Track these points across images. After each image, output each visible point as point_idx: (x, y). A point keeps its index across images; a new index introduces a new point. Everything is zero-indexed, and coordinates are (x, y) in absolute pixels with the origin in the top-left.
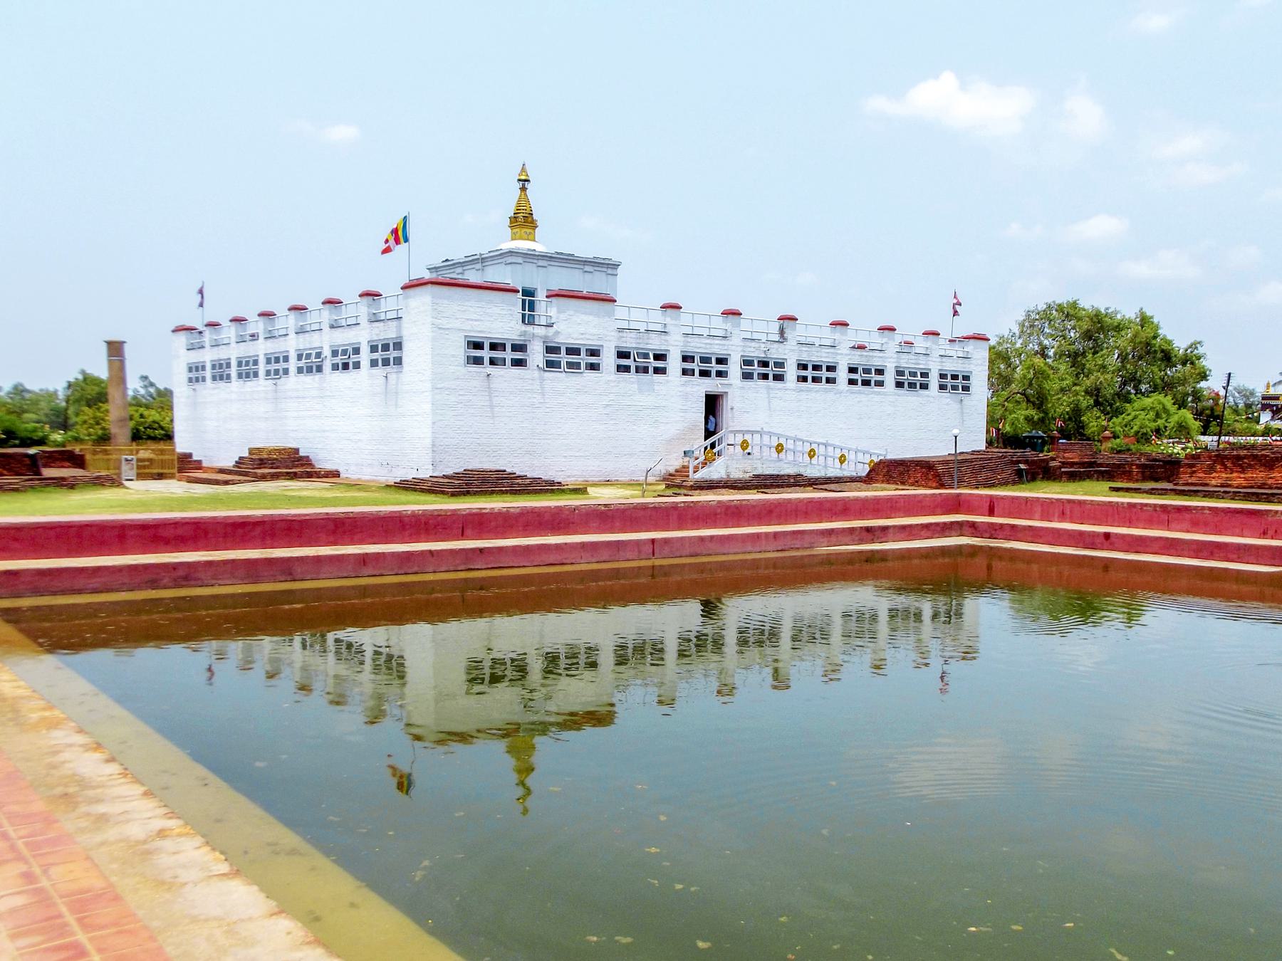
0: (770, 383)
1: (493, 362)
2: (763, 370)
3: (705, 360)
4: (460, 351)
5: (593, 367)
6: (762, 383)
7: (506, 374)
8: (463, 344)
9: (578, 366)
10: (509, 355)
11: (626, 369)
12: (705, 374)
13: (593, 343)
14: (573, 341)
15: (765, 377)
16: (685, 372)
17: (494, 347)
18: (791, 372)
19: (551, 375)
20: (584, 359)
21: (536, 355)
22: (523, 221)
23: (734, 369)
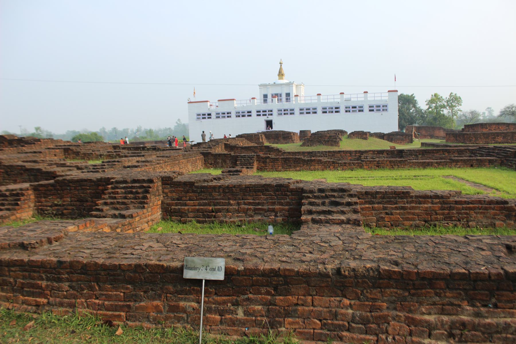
0: (289, 116)
1: (203, 118)
2: (286, 112)
3: (263, 111)
4: (196, 117)
5: (230, 117)
6: (286, 116)
7: (207, 121)
8: (196, 115)
9: (225, 117)
10: (207, 116)
11: (239, 116)
12: (263, 115)
13: (229, 111)
14: (223, 111)
15: (288, 114)
16: (258, 115)
17: (203, 115)
18: (297, 112)
19: (218, 120)
20: (226, 115)
21: (213, 116)
22: (281, 74)
23: (275, 113)
